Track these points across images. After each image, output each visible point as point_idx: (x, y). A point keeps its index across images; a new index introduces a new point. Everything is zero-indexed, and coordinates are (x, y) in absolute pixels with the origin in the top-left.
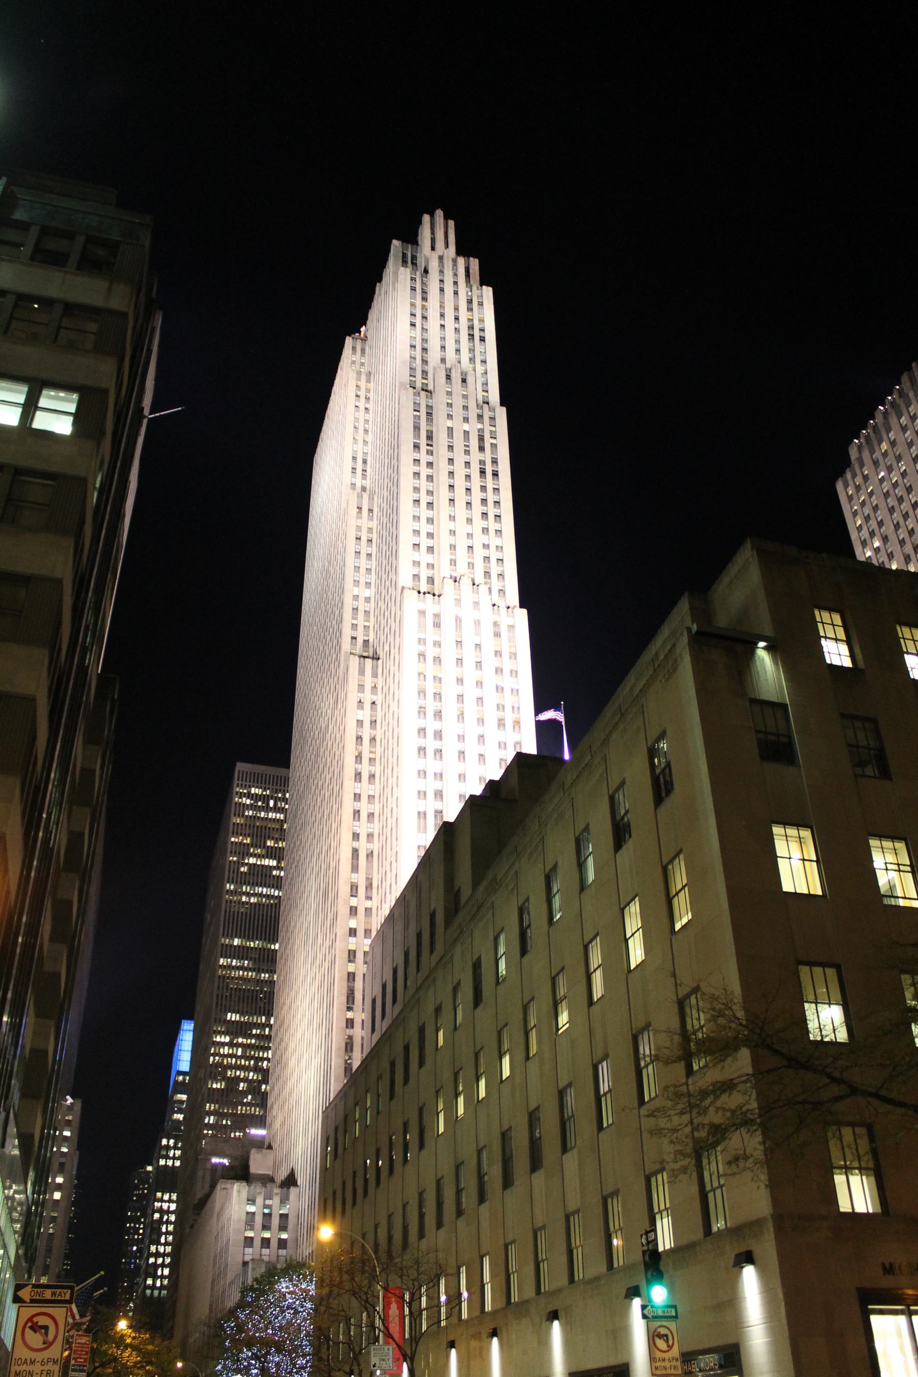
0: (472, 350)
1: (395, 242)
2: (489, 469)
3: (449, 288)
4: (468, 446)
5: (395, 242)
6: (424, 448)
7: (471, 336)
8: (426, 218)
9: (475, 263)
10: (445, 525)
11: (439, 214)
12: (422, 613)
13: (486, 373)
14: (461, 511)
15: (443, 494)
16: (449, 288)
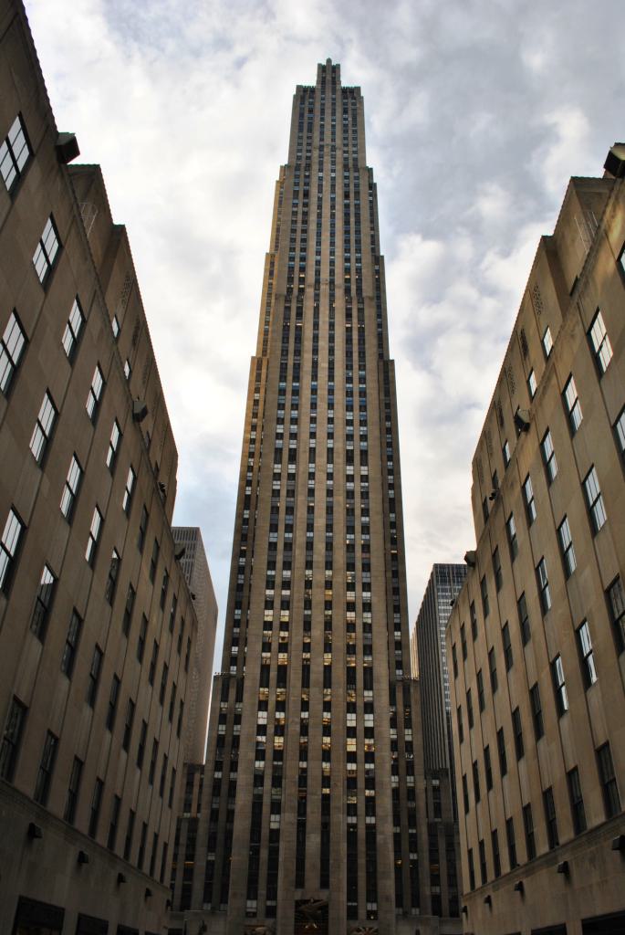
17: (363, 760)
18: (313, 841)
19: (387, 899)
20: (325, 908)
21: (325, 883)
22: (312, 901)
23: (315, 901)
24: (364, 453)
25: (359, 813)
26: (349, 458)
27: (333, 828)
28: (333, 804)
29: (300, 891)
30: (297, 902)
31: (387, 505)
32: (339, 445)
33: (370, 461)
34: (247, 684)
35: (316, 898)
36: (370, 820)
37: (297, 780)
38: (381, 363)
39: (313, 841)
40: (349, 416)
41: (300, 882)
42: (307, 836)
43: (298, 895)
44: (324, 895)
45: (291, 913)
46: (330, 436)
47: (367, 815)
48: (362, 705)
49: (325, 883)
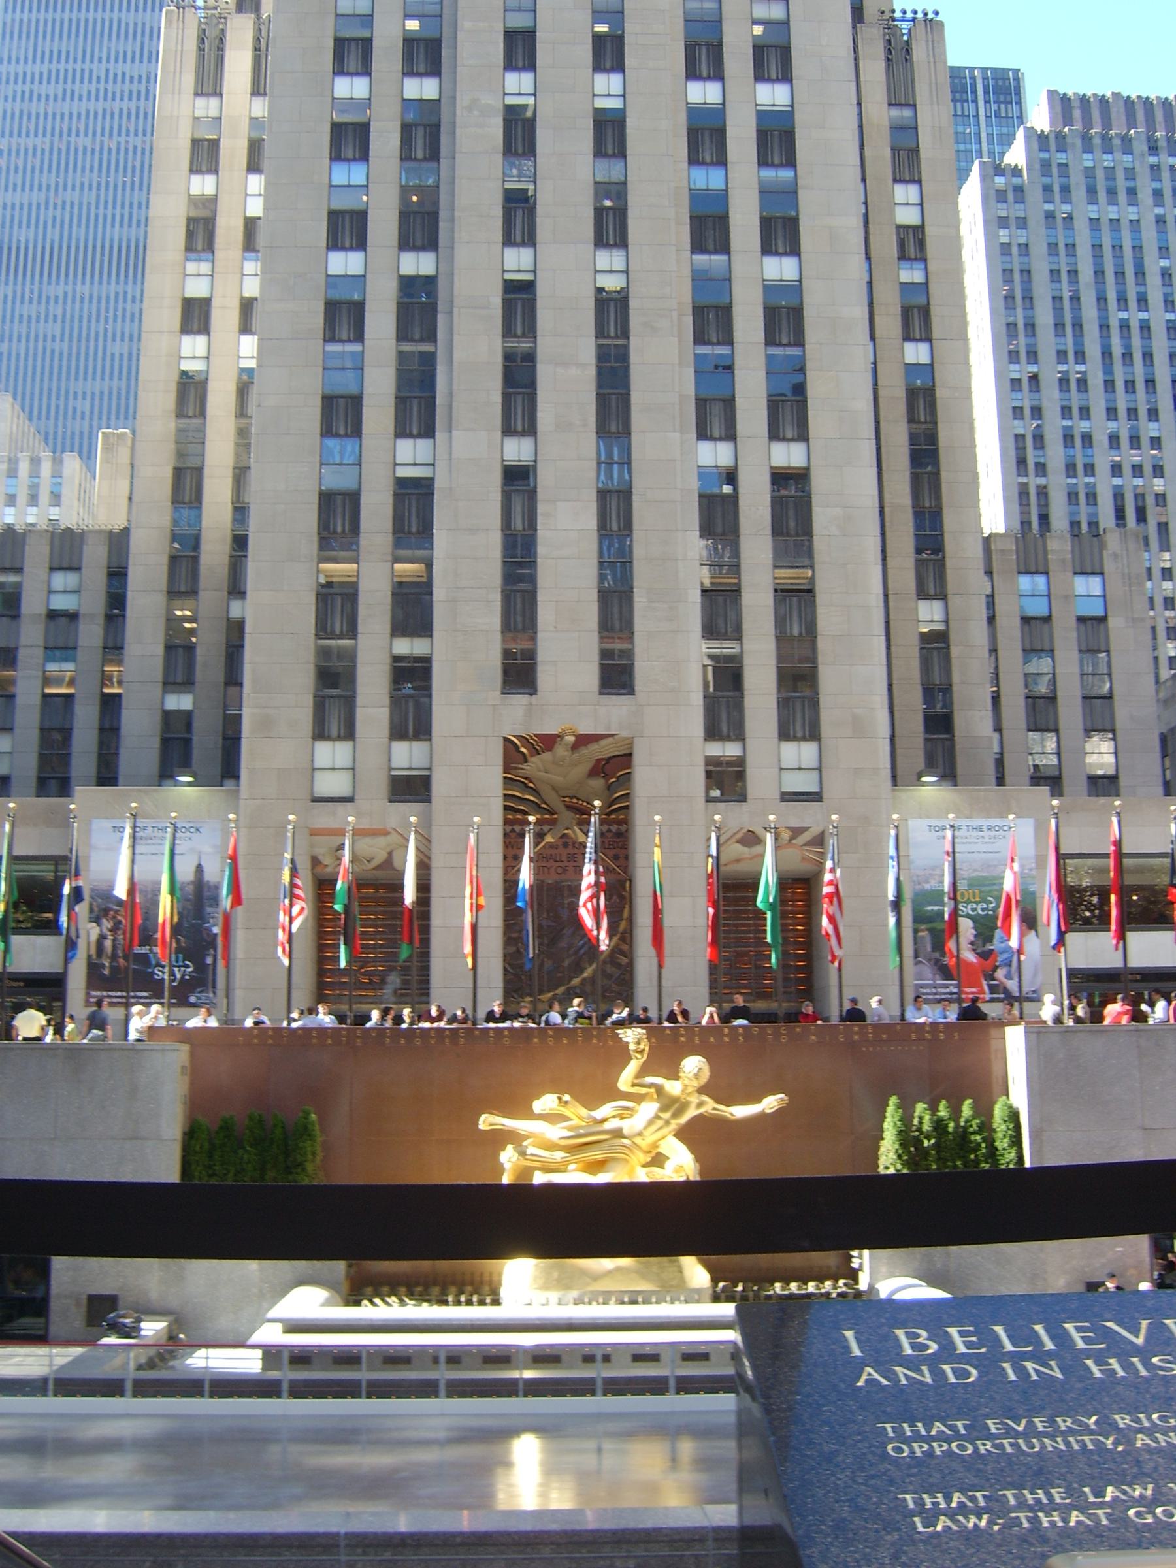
19: (859, 728)
20: (615, 768)
21: (617, 676)
22: (571, 739)
23: (584, 740)
25: (741, 428)
29: (520, 701)
35: (586, 728)
36: (788, 455)
41: (519, 674)
42: (541, 508)
43: (516, 716)
44: (609, 716)
45: (491, 780)
47: (775, 434)
49: (617, 676)
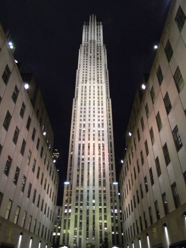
0: (97, 37)
1: (85, 22)
2: (99, 58)
3: (93, 27)
4: (94, 54)
5: (85, 22)
6: (86, 56)
7: (97, 35)
8: (90, 16)
9: (101, 23)
10: (89, 69)
11: (93, 15)
12: (83, 86)
13: (100, 41)
14: (92, 67)
15: (89, 64)
16: (93, 27)
17: (103, 205)
18: (91, 227)
24: (103, 124)
26: (99, 126)
27: (96, 224)
28: (96, 217)
30: (87, 244)
31: (109, 137)
32: (96, 123)
33: (104, 127)
34: (73, 186)
37: (86, 211)
38: (107, 100)
39: (91, 227)
40: (99, 115)
43: (87, 242)
46: (94, 120)
48: (103, 191)
